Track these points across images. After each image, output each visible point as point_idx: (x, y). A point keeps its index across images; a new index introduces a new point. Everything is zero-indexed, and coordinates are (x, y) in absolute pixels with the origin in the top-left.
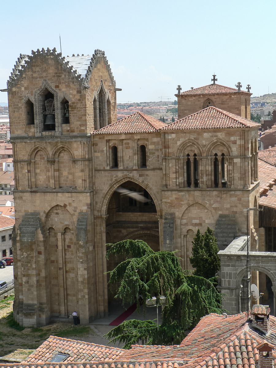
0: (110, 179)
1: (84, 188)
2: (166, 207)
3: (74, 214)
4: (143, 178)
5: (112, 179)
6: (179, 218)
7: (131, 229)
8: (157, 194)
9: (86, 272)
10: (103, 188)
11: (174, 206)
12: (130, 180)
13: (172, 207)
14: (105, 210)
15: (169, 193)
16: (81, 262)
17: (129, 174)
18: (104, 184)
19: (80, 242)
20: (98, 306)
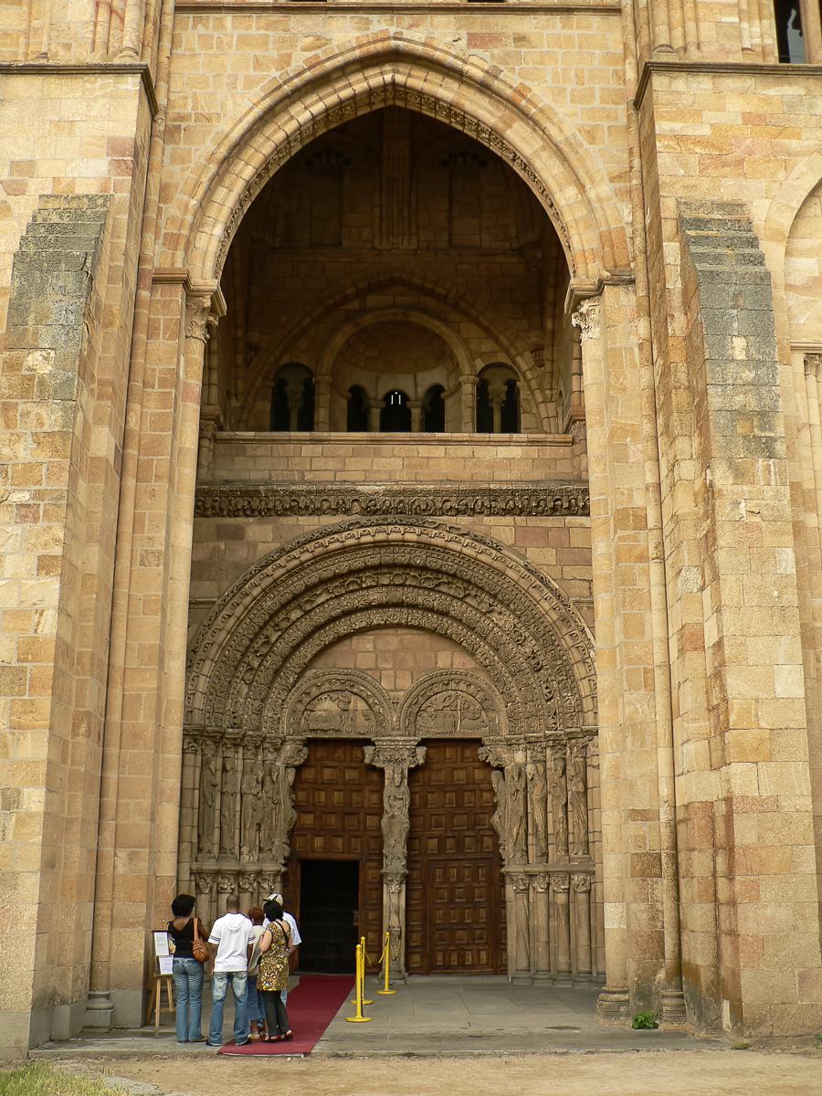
0: (274, 54)
1: (100, 51)
2: (685, 166)
3: (9, 209)
4: (496, 52)
5: (289, 56)
6: (775, 236)
7: (303, 520)
8: (586, 145)
9: (51, 588)
10: (223, 105)
11: (740, 162)
12: (400, 79)
13: (727, 169)
14: (214, 246)
15: (704, 83)
16: (21, 506)
17: (405, 32)
18: (233, 85)
19: (34, 359)
20: (104, 930)
